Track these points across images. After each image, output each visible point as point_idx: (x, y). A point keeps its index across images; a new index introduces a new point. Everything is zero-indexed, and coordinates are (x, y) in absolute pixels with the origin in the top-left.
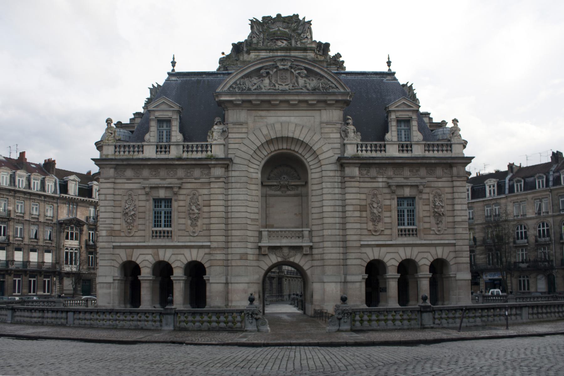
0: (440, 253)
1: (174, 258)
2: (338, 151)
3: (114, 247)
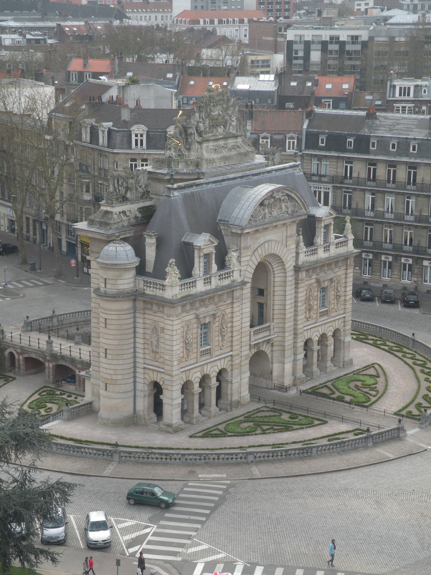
0: (337, 325)
1: (212, 370)
2: (294, 259)
3: (182, 372)
